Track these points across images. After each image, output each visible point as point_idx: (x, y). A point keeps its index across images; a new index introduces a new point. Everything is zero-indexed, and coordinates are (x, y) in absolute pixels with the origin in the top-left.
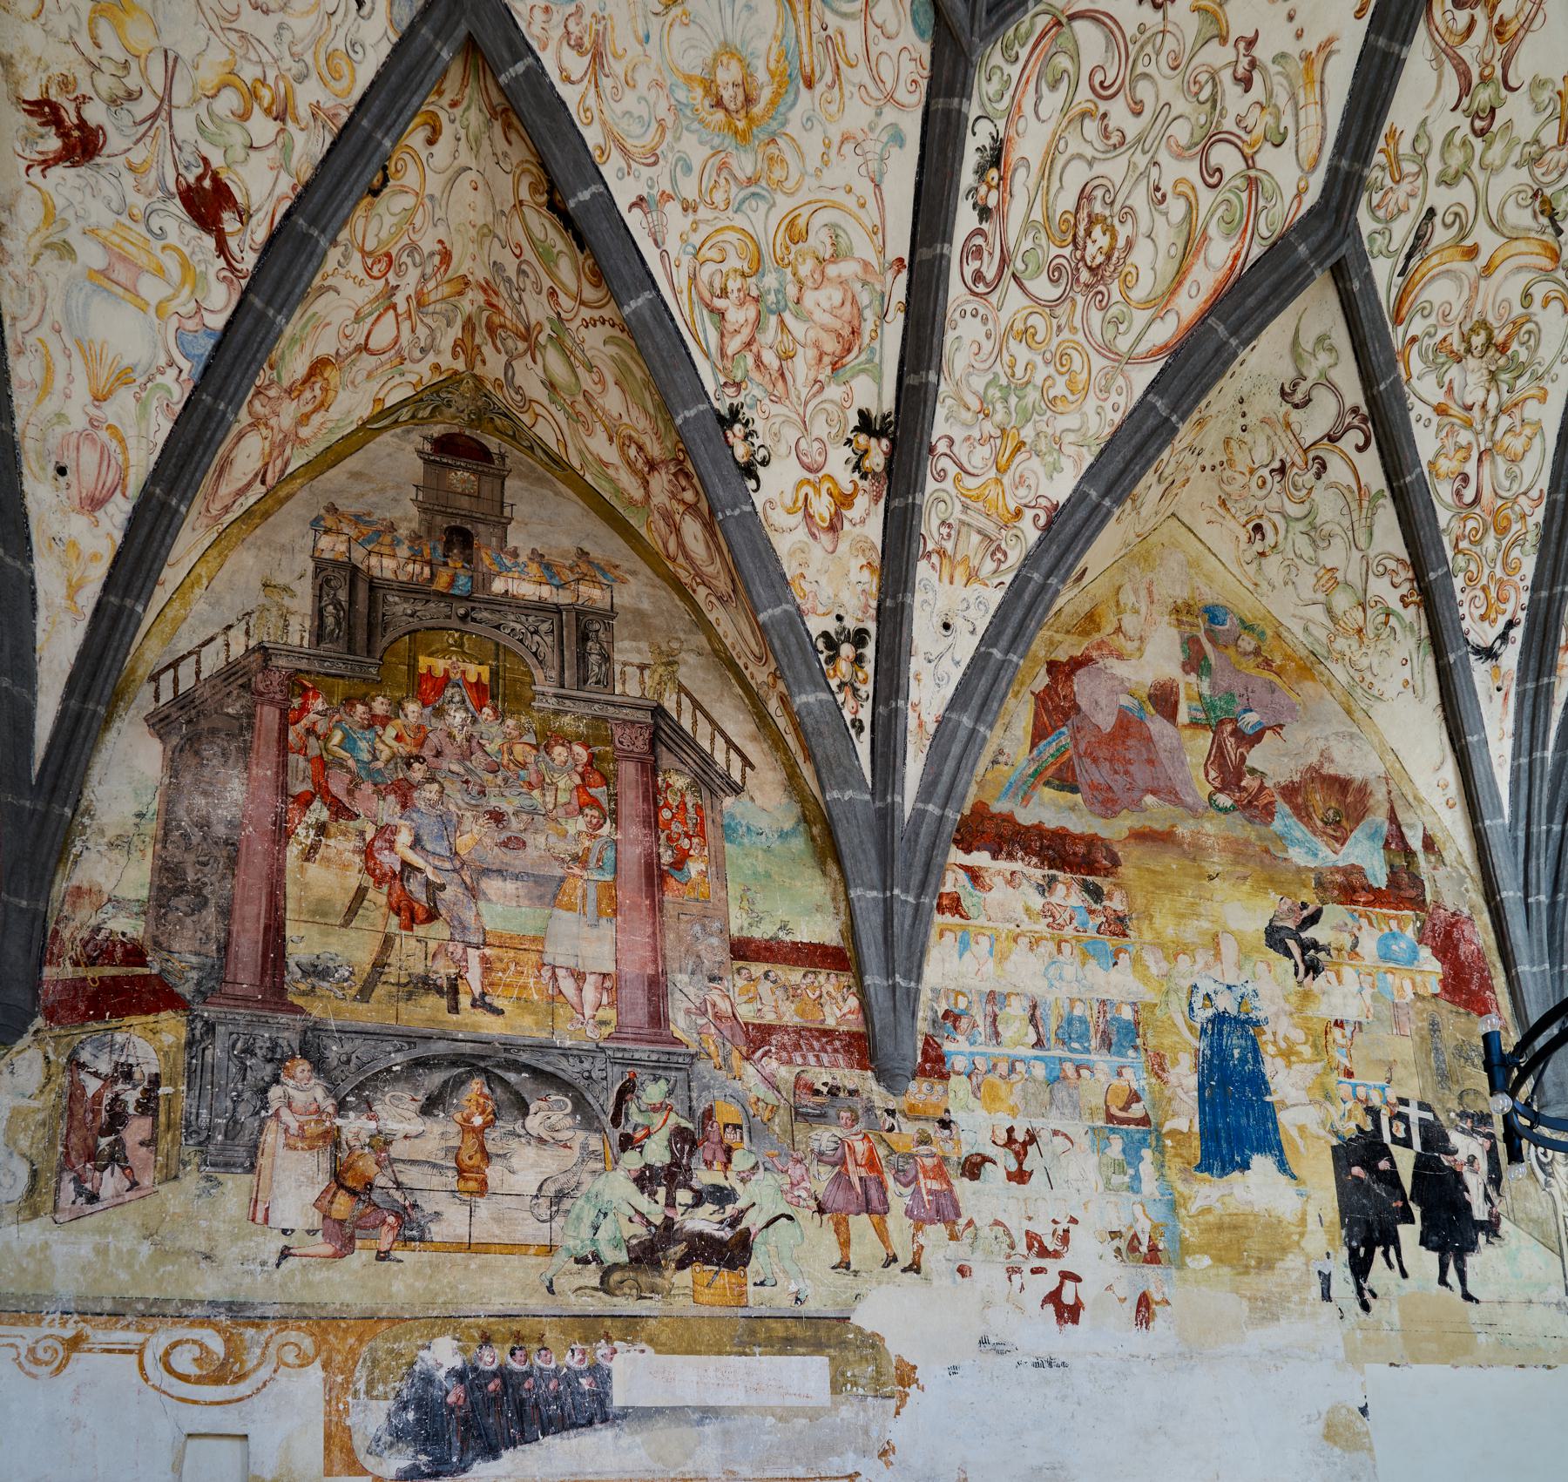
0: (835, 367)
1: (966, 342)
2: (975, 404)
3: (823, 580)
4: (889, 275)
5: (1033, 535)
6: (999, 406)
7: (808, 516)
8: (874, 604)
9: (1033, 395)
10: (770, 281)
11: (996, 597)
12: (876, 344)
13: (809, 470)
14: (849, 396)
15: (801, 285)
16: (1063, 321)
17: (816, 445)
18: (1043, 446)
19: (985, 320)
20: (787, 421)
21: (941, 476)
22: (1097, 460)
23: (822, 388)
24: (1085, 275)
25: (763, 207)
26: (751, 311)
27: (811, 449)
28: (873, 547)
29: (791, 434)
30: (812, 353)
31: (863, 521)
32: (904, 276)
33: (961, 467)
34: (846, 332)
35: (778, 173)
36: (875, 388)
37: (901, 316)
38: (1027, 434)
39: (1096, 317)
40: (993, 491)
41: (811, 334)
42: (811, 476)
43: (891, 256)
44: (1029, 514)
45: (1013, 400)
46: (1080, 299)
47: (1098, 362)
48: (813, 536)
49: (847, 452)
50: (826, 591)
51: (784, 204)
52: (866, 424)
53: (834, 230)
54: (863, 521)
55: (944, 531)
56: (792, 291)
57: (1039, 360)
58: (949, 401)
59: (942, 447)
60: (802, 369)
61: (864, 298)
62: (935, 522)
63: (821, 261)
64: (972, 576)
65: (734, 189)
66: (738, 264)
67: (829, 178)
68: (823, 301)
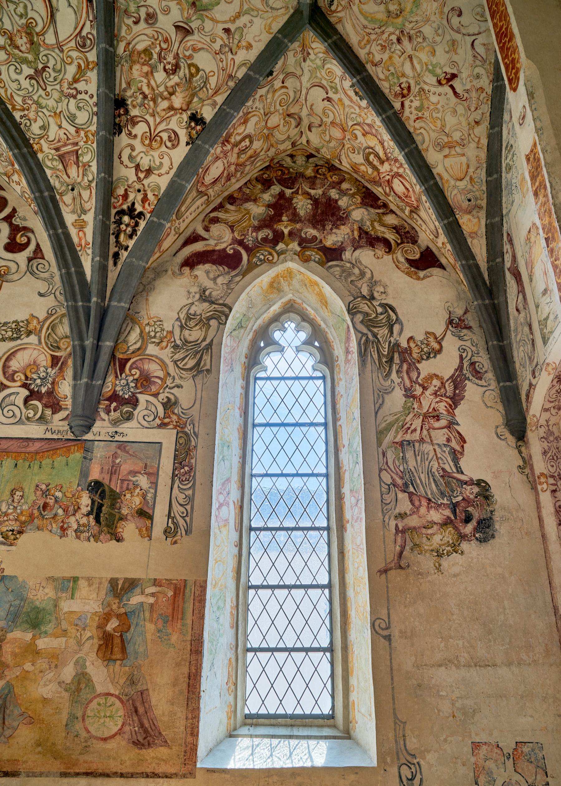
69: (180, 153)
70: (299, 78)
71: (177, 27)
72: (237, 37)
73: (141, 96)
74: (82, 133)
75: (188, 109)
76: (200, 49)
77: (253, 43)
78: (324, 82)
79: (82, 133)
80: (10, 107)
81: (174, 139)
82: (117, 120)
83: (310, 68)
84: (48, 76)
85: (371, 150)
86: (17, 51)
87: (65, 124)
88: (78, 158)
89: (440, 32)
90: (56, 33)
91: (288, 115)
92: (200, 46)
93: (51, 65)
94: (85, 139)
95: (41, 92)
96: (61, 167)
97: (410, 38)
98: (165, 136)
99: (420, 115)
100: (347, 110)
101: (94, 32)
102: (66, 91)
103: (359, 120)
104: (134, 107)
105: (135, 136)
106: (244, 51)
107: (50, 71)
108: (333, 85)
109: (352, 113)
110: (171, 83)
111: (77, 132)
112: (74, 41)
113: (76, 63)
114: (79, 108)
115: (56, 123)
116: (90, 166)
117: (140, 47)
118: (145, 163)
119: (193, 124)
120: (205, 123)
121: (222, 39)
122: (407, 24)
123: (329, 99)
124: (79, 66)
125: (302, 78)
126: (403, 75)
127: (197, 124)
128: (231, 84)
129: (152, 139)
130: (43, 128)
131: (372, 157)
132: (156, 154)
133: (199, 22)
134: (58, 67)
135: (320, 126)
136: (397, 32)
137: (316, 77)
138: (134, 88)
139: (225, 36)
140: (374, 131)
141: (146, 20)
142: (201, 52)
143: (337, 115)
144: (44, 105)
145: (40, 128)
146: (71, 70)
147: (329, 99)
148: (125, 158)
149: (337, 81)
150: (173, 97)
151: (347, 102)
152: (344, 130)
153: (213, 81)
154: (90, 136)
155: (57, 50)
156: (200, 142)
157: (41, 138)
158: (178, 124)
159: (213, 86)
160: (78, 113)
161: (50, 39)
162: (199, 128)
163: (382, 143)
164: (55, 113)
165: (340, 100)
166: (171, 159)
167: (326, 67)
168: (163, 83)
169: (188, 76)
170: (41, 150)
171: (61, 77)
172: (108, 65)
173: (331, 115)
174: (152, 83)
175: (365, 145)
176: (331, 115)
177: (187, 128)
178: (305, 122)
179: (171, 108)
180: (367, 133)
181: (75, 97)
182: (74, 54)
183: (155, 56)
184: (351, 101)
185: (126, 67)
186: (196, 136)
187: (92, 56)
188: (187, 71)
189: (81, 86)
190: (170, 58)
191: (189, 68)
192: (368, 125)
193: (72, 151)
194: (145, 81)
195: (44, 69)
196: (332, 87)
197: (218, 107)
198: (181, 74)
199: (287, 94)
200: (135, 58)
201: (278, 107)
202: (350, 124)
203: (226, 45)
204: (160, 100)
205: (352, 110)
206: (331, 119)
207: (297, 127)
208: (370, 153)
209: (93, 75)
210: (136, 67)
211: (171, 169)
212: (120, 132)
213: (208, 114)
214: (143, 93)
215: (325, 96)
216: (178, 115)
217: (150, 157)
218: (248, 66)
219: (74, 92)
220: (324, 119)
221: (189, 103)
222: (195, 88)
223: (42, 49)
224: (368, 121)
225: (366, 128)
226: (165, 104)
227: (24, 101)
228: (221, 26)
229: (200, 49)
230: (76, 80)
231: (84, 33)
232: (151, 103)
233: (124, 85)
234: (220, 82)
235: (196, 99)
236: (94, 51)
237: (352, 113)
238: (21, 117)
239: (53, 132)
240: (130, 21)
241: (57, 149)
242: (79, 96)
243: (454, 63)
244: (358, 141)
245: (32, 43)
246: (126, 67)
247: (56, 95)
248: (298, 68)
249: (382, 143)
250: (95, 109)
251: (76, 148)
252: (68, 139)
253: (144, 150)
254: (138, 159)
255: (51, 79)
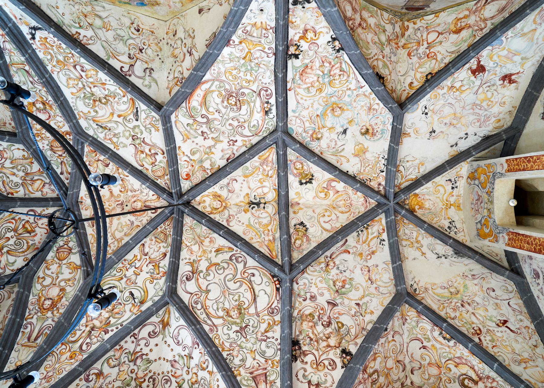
0: (307, 66)
1: (267, 78)
2: (261, 66)
3: (309, 17)
4: (292, 87)
5: (234, 38)
6: (254, 66)
7: (315, 32)
8: (290, 13)
9: (243, 69)
10: (326, 80)
11: (244, 20)
12: (294, 73)
13: (314, 43)
14: (302, 61)
15: (318, 81)
16: (238, 85)
17: (312, 49)
18: (236, 59)
19: (262, 83)
20: (321, 53)
21: (269, 49)
22: (217, 58)
23: (310, 62)
24: (234, 95)
25: (329, 93)
26: (332, 73)
27: (313, 47)
28: (291, 28)
29: (320, 50)
30: (314, 68)
31: (296, 34)
32: (288, 88)
33: (263, 51)
34: (304, 74)
35: (325, 100)
36: (294, 64)
37: (288, 80)
38: (242, 61)
39: (227, 87)
40: (251, 47)
41: (314, 72)
42: (314, 41)
43: (293, 91)
44: (237, 43)
45: (249, 68)
46: (234, 90)
47: (224, 78)
48: (313, 27)
49: (302, 49)
50: (308, 14)
51: (323, 94)
52: (296, 56)
53: (309, 91)
54: (296, 34)
55: (266, 35)
56: (320, 79)
57: (243, 77)
58: (270, 65)
59: (271, 55)
60: (317, 64)
61: (299, 82)
62: (270, 37)
63: (312, 86)
64: (254, 25)
65: (337, 95)
66: (336, 81)
67: (312, 101)
68: (311, 78)
69: (338, 373)
70: (401, 335)
71: (328, 303)
72: (364, 307)
73: (309, 339)
74: (270, 362)
75: (339, 346)
76: (343, 314)
77: (374, 311)
78: (419, 336)
79: (270, 362)
80: (220, 349)
81: (333, 364)
82: (294, 353)
83: (408, 329)
84: (248, 330)
85: (464, 376)
86: (230, 319)
87: (258, 357)
88: (266, 378)
89: (486, 299)
90: (256, 308)
91: (398, 361)
92: (342, 312)
93: (251, 324)
94: (271, 365)
95: (243, 339)
96: (253, 384)
97: (469, 304)
98: (326, 362)
99: (494, 344)
100: (439, 351)
101: (280, 306)
102: (259, 338)
103: (450, 356)
104: (305, 345)
105: (306, 363)
106: (369, 315)
107: (250, 327)
108: (426, 336)
109: (444, 353)
110: (326, 332)
111: (266, 361)
112: (266, 311)
113: (267, 322)
114: (268, 347)
115: (252, 357)
116: (275, 383)
117: (307, 312)
118: (315, 380)
119: (344, 355)
120: (352, 355)
121: (355, 309)
122: (464, 297)
123: (424, 347)
124: (269, 324)
125: (403, 336)
126: (473, 323)
127: (347, 355)
128: (365, 333)
129: (318, 364)
130: (242, 360)
131: (466, 382)
132: (322, 374)
133: (341, 300)
134: (255, 325)
135: (420, 368)
136: (460, 302)
137: (413, 334)
138: (304, 335)
139: (357, 307)
140: (464, 361)
141: (310, 299)
142: (344, 316)
143: (432, 357)
144: (244, 347)
145: (240, 361)
146: (264, 326)
147: (424, 347)
148: (300, 376)
149: (429, 333)
150: (329, 340)
151: (438, 346)
152: (439, 367)
153: (353, 331)
154: (276, 363)
155: (256, 316)
156: (352, 365)
157: (240, 367)
158: (335, 355)
159: (354, 334)
160: (267, 350)
161: (252, 310)
162: (348, 357)
163: (472, 368)
164: (251, 351)
165: (433, 346)
166: (332, 377)
167: (419, 326)
168: (322, 332)
169: (337, 328)
170: (240, 375)
171: (257, 330)
172: (289, 320)
173: (428, 358)
174: (315, 331)
175: (459, 374)
176: (428, 358)
177: (341, 358)
178: (408, 368)
179: (329, 346)
180: (458, 364)
181: (265, 341)
182: (266, 318)
183: (316, 317)
184: (441, 344)
185: (299, 323)
186: (347, 363)
187: (278, 318)
188: (336, 326)
189: (269, 334)
190: (325, 318)
191: (337, 324)
192: (458, 358)
193: (263, 374)
194: (311, 331)
195: (246, 327)
196: (425, 338)
197: (359, 346)
198: (333, 327)
199: (395, 346)
200: (304, 318)
201: (391, 354)
202: (443, 361)
203: (358, 312)
204: (321, 341)
205: (444, 351)
206: (427, 362)
207: (403, 371)
208: (464, 379)
209: (278, 328)
210: (305, 323)
211: (333, 383)
212: (296, 360)
213: (353, 349)
214: (310, 337)
215: (421, 345)
216: (334, 350)
217: (318, 376)
218: (373, 323)
219: (265, 338)
220: (423, 363)
221: (340, 343)
222: (342, 335)
223: (246, 316)
224: (458, 355)
225: (457, 360)
226: (325, 344)
227: (231, 346)
228: (354, 302)
229: (343, 314)
230: (266, 331)
231: (273, 306)
232: (316, 343)
233: (297, 333)
234: (357, 332)
235: (343, 341)
236: (279, 315)
237: (444, 353)
238: (228, 355)
239: (249, 362)
240: (301, 300)
241: (251, 373)
242: (268, 340)
243: (502, 315)
244: (452, 373)
245: (240, 313)
246: (299, 323)
247: (253, 340)
248: (401, 329)
249: (472, 368)
250: (279, 347)
251: (265, 371)
252: (259, 366)
253: (313, 371)
254: (309, 377)
255: (251, 332)
